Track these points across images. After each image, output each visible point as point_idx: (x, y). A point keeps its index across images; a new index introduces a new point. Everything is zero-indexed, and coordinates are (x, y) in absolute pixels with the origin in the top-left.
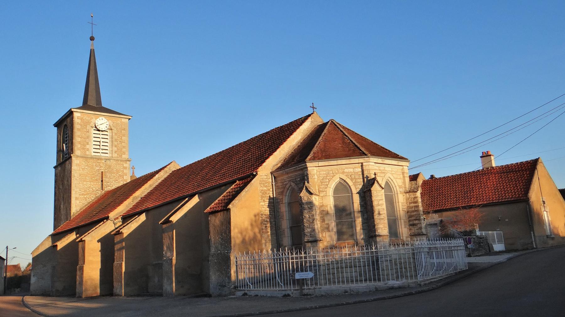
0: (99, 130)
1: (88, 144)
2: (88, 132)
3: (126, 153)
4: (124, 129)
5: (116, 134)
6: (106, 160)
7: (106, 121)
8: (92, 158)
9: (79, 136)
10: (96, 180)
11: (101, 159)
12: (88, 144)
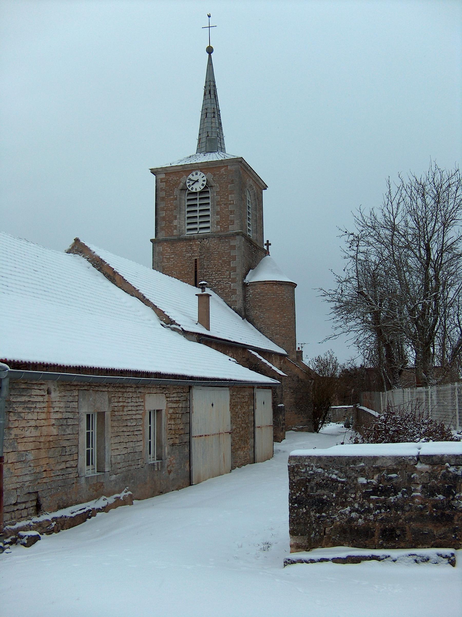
0: (195, 193)
1: (176, 218)
2: (176, 199)
3: (236, 222)
4: (232, 182)
5: (218, 193)
6: (206, 237)
7: (203, 175)
8: (181, 240)
9: (163, 209)
10: (187, 274)
11: (194, 239)
12: (176, 218)
